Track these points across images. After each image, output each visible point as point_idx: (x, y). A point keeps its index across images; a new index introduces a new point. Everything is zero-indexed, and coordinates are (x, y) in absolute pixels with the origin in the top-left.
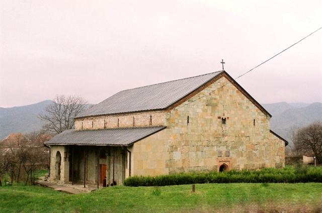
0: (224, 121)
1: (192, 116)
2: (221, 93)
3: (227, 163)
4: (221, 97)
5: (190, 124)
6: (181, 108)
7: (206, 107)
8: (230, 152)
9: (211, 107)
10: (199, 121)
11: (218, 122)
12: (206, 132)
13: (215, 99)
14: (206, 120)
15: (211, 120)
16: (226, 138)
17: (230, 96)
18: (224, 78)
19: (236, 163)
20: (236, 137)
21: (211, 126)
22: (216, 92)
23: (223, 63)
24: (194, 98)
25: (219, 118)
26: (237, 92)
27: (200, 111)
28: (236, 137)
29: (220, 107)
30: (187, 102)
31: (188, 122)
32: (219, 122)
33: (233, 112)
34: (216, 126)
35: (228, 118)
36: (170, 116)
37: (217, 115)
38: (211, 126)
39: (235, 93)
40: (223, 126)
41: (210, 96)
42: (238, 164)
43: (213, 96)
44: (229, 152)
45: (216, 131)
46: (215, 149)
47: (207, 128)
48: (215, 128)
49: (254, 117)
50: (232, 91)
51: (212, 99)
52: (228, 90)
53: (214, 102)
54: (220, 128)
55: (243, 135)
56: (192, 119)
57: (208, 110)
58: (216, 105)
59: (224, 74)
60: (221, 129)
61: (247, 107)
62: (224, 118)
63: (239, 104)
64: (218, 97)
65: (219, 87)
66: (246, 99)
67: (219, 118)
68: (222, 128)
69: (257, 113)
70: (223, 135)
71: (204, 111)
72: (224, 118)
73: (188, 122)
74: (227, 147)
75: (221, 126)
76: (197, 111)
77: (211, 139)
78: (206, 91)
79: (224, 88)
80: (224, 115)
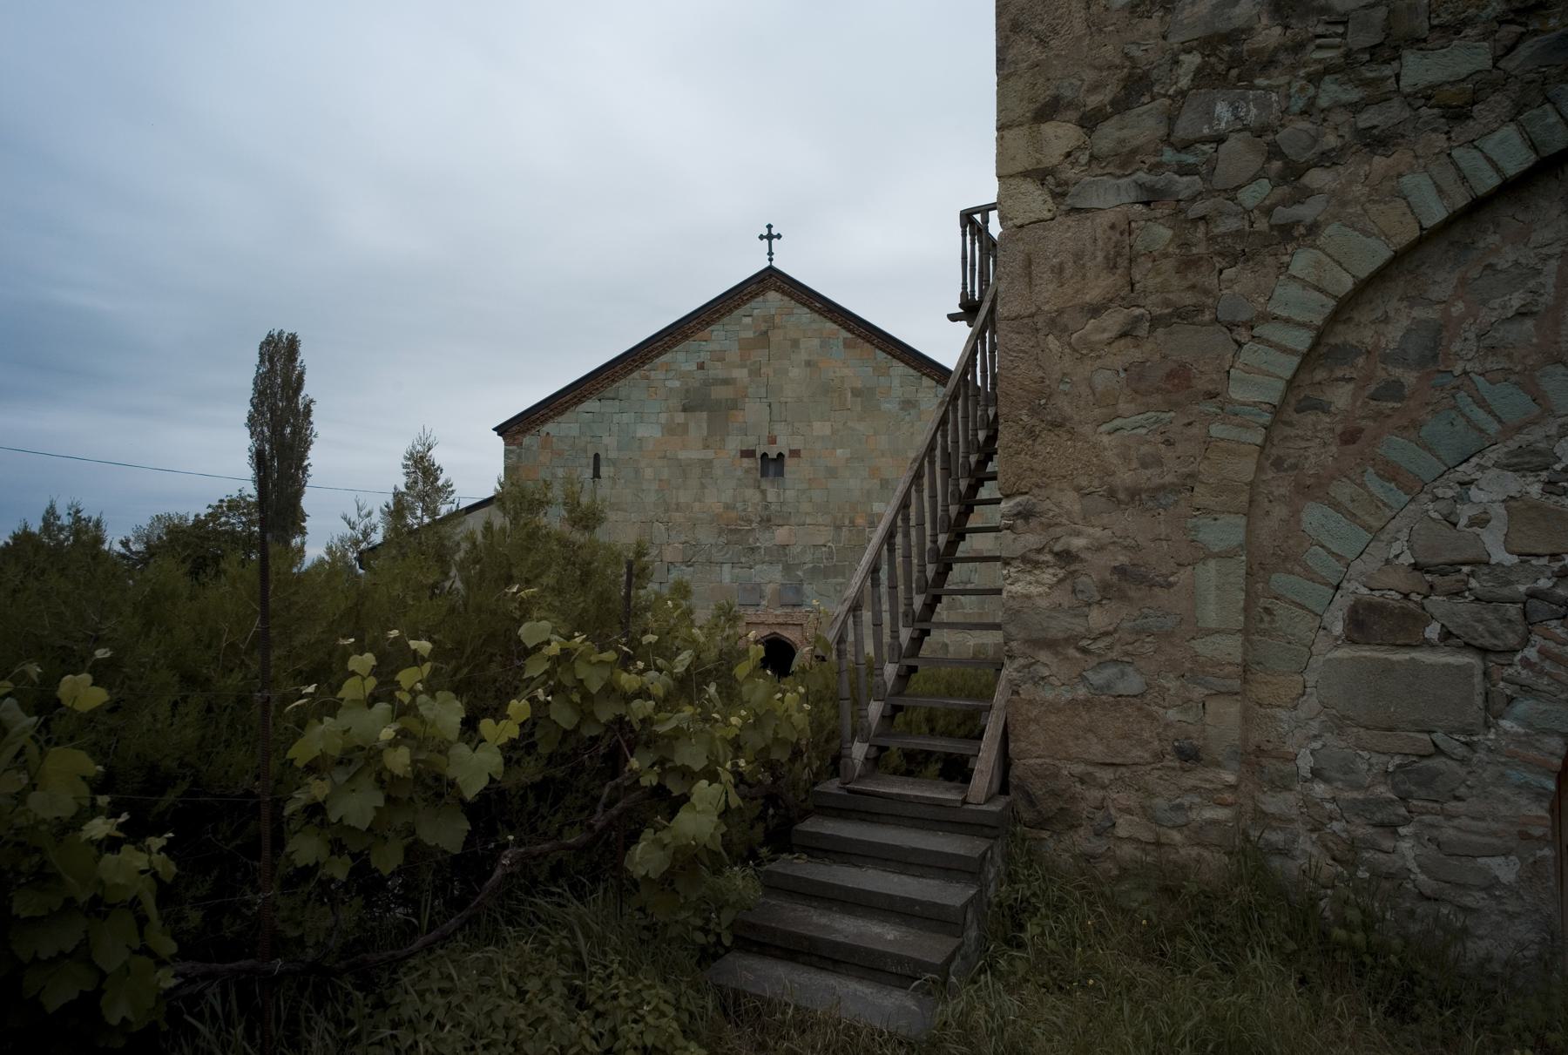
0: (772, 465)
1: (613, 455)
2: (759, 355)
3: (790, 635)
4: (755, 372)
5: (604, 482)
6: (560, 428)
7: (680, 417)
8: (807, 588)
9: (705, 415)
10: (648, 473)
11: (739, 473)
12: (677, 510)
13: (726, 382)
15: (708, 464)
16: (781, 535)
17: (808, 364)
18: (773, 297)
20: (838, 528)
21: (703, 486)
22: (734, 355)
23: (770, 237)
24: (623, 387)
25: (748, 454)
26: (847, 344)
27: (649, 432)
28: (838, 528)
29: (754, 411)
30: (591, 405)
31: (597, 475)
32: (747, 471)
33: (821, 428)
34: (730, 489)
35: (795, 453)
36: (519, 456)
37: (734, 444)
38: (703, 486)
40: (765, 484)
41: (700, 374)
43: (717, 371)
44: (798, 590)
45: (727, 507)
46: (727, 574)
47: (683, 497)
48: (727, 497)
50: (816, 342)
51: (708, 383)
52: (795, 344)
53: (719, 393)
54: (752, 495)
56: (613, 463)
57: (692, 425)
58: (734, 405)
59: (770, 279)
60: (757, 497)
63: (856, 393)
64: (741, 374)
65: (750, 334)
66: (899, 368)
67: (748, 454)
68: (763, 492)
70: (767, 522)
71: (670, 429)
73: (597, 475)
74: (788, 568)
76: (639, 435)
77: (706, 536)
78: (681, 359)
79: (776, 337)
80: (773, 441)
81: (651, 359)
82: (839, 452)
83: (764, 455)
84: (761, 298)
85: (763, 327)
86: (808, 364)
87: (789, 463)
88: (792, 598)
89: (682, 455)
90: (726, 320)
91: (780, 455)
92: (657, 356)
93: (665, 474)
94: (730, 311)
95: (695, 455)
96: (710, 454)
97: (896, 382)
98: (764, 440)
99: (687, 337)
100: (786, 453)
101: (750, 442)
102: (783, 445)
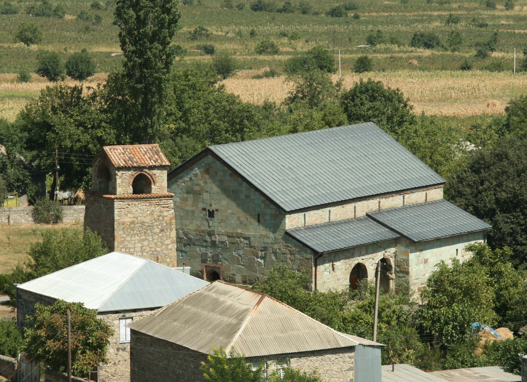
0: (211, 214)
7: (186, 195)
9: (192, 195)
14: (187, 212)
15: (193, 212)
17: (220, 180)
19: (230, 271)
25: (204, 209)
35: (217, 210)
37: (201, 206)
39: (228, 178)
42: (231, 273)
49: (258, 210)
50: (222, 173)
52: (216, 173)
53: (197, 188)
55: (239, 236)
57: (189, 199)
61: (247, 197)
62: (211, 210)
63: (233, 192)
67: (204, 209)
69: (263, 206)
72: (211, 210)
75: (207, 220)
80: (211, 205)
81: (177, 175)
82: (229, 211)
83: (209, 210)
84: (206, 157)
85: (207, 167)
86: (220, 180)
87: (215, 213)
88: (215, 259)
89: (186, 208)
90: (197, 163)
91: (213, 211)
92: (179, 174)
93: (182, 214)
94: (198, 161)
95: (189, 208)
96: (194, 208)
97: (244, 189)
98: (208, 205)
99: (186, 169)
100: (215, 210)
101: (204, 206)
102: (214, 207)
